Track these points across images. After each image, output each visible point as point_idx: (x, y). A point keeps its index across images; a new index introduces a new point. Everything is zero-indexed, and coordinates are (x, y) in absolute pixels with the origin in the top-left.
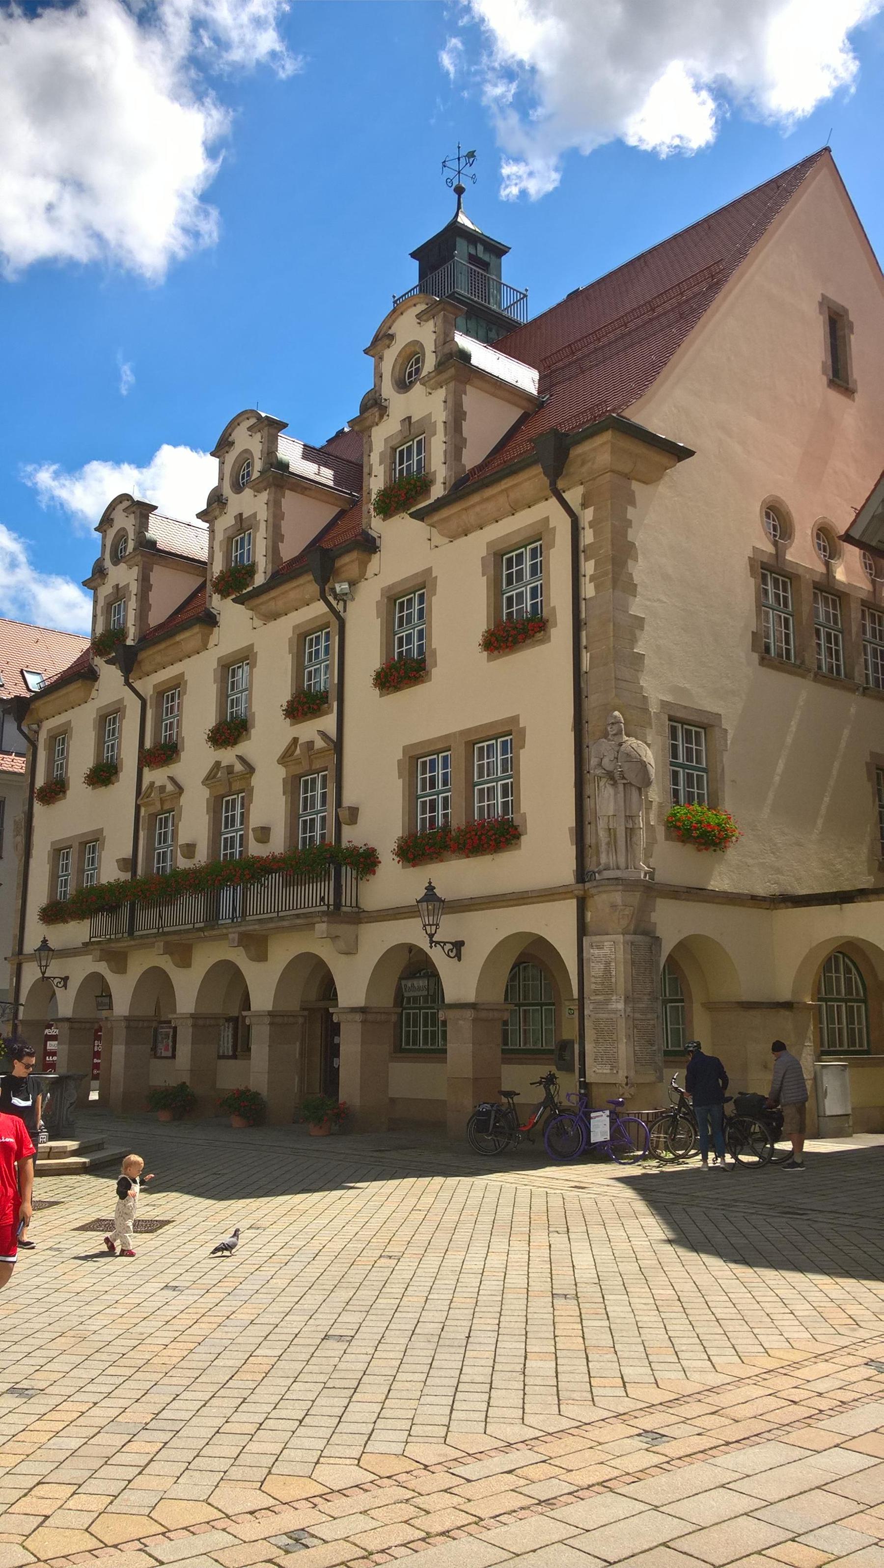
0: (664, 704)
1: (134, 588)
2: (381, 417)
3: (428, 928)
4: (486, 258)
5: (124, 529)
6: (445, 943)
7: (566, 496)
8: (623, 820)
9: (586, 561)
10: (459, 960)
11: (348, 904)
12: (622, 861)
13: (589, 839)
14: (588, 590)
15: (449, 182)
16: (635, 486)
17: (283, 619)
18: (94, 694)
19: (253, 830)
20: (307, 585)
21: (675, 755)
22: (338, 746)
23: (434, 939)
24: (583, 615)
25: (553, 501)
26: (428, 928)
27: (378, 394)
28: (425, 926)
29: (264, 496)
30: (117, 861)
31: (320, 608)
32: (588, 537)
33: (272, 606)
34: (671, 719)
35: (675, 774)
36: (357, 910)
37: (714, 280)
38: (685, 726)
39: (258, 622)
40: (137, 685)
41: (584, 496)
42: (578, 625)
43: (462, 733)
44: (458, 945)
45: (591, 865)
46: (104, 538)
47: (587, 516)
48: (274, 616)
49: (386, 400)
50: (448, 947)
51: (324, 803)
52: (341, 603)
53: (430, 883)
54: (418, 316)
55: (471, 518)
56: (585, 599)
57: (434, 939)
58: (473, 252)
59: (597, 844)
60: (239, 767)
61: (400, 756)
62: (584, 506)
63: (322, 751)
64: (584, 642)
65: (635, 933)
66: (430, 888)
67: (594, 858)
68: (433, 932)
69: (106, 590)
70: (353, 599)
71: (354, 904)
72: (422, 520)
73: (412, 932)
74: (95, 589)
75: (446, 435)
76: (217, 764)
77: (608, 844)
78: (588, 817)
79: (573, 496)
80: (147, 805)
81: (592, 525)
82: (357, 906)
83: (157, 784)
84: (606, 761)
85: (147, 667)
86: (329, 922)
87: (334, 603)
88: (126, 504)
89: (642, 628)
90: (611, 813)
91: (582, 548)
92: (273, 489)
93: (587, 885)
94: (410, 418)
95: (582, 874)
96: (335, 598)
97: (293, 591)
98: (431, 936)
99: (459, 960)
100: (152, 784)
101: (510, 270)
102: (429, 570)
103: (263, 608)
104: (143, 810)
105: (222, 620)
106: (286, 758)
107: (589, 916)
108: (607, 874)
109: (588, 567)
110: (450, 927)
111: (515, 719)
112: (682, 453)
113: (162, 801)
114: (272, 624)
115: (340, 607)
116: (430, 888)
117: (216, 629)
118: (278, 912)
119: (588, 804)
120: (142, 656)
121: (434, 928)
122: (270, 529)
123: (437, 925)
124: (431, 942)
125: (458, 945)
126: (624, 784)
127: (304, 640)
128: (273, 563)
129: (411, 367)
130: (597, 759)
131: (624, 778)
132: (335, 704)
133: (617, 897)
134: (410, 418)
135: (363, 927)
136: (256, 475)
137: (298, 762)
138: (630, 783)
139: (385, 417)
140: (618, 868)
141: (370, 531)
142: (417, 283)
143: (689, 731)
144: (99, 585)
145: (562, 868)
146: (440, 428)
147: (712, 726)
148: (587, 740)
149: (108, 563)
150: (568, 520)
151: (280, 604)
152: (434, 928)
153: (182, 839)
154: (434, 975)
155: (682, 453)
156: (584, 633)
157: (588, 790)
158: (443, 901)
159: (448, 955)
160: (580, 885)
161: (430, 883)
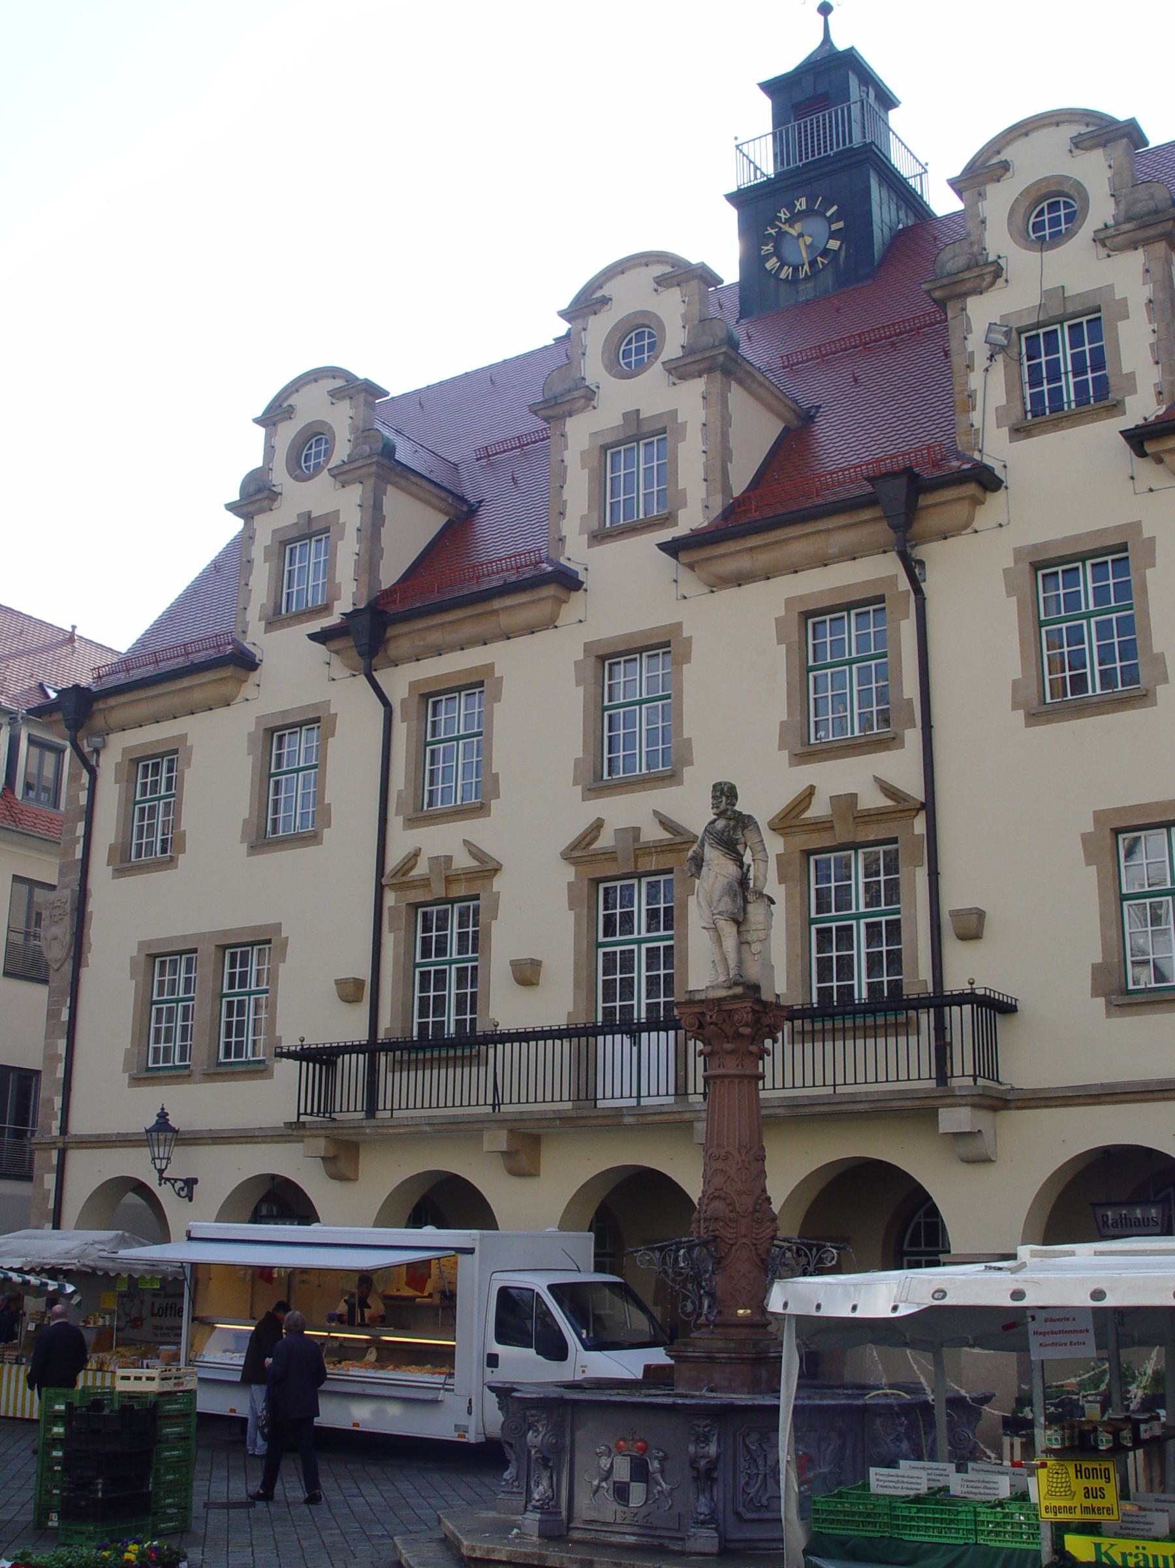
3: (158, 1161)
6: (176, 1180)
10: (191, 1200)
26: (158, 1161)
28: (154, 1159)
44: (191, 1183)
50: (180, 1184)
53: (163, 1109)
66: (163, 1115)
73: (137, 1164)
98: (161, 1171)
99: (191, 1200)
110: (183, 1162)
116: (163, 1115)
121: (164, 1161)
123: (169, 1159)
124: (161, 1178)
125: (191, 1183)
152: (164, 1161)
158: (177, 1132)
159: (179, 1195)
161: (163, 1109)
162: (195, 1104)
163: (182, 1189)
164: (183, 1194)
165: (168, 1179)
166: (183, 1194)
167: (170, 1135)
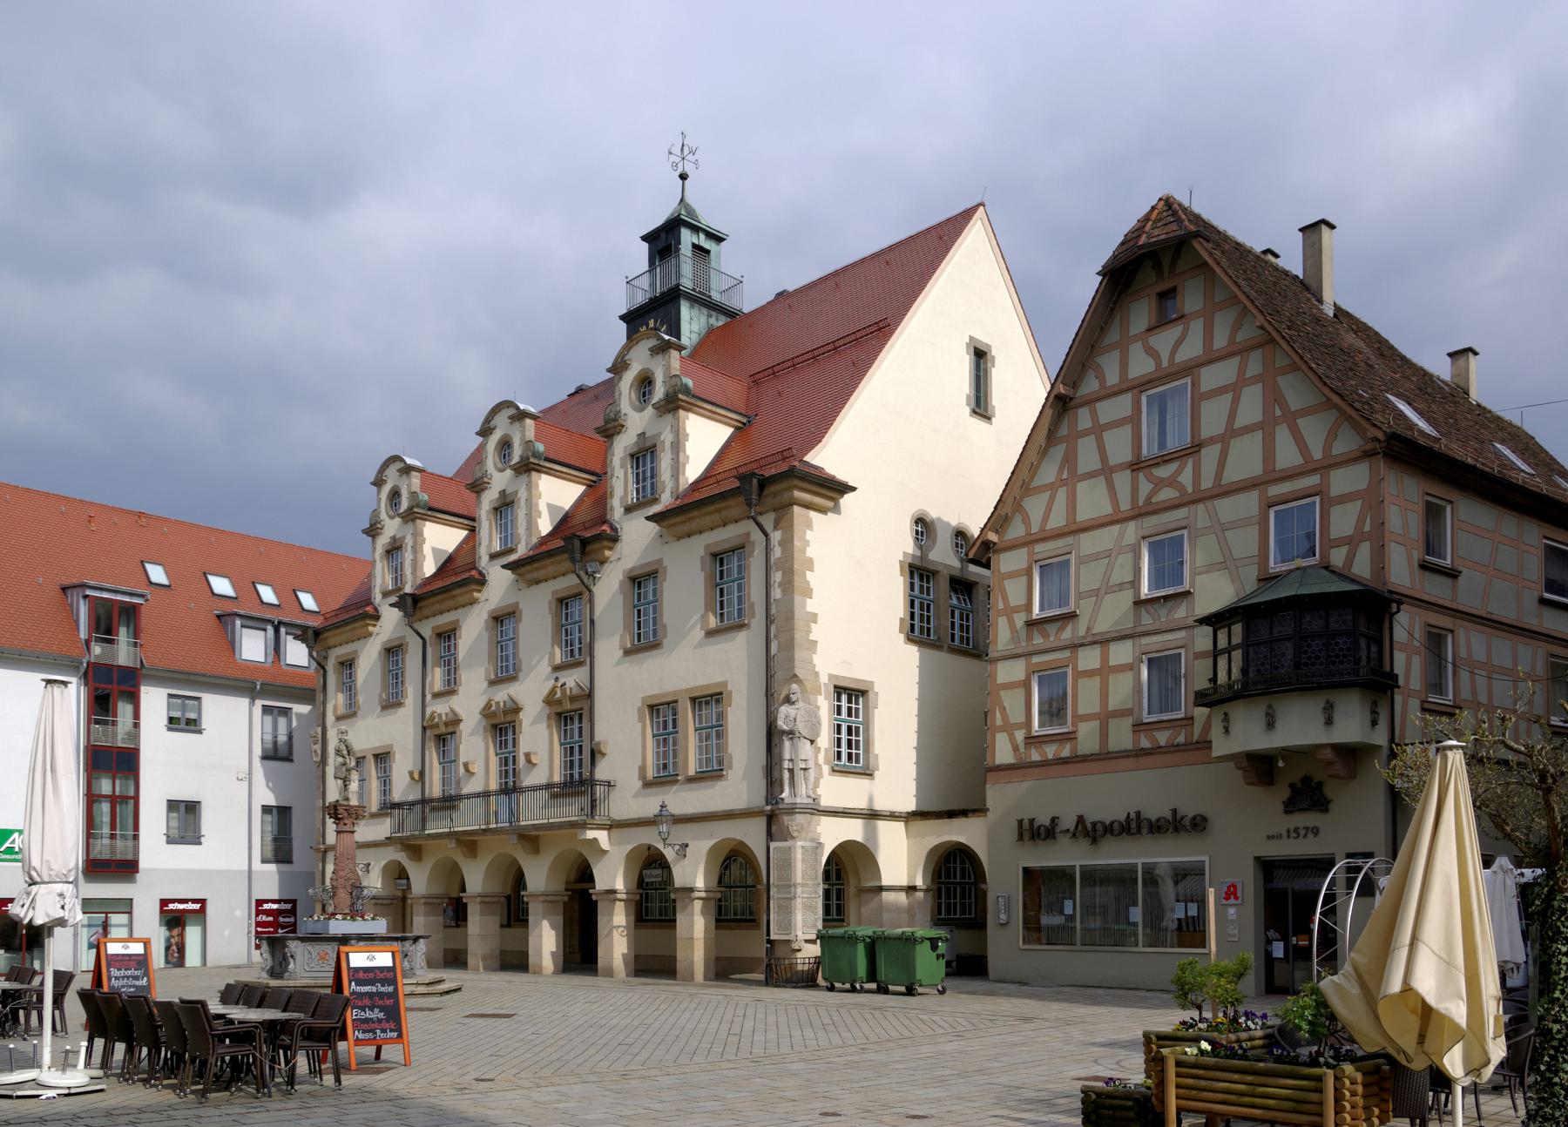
0: (831, 677)
22: (589, 695)
33: (535, 575)
34: (836, 687)
35: (839, 726)
37: (879, 331)
39: (522, 585)
42: (769, 620)
43: (686, 690)
48: (537, 582)
51: (580, 735)
54: (651, 350)
55: (693, 525)
69: (383, 540)
97: (551, 567)
101: (725, 258)
103: (529, 576)
111: (725, 684)
114: (534, 587)
127: (563, 602)
143: (852, 695)
153: (462, 760)
157: (775, 739)
162: (684, 800)
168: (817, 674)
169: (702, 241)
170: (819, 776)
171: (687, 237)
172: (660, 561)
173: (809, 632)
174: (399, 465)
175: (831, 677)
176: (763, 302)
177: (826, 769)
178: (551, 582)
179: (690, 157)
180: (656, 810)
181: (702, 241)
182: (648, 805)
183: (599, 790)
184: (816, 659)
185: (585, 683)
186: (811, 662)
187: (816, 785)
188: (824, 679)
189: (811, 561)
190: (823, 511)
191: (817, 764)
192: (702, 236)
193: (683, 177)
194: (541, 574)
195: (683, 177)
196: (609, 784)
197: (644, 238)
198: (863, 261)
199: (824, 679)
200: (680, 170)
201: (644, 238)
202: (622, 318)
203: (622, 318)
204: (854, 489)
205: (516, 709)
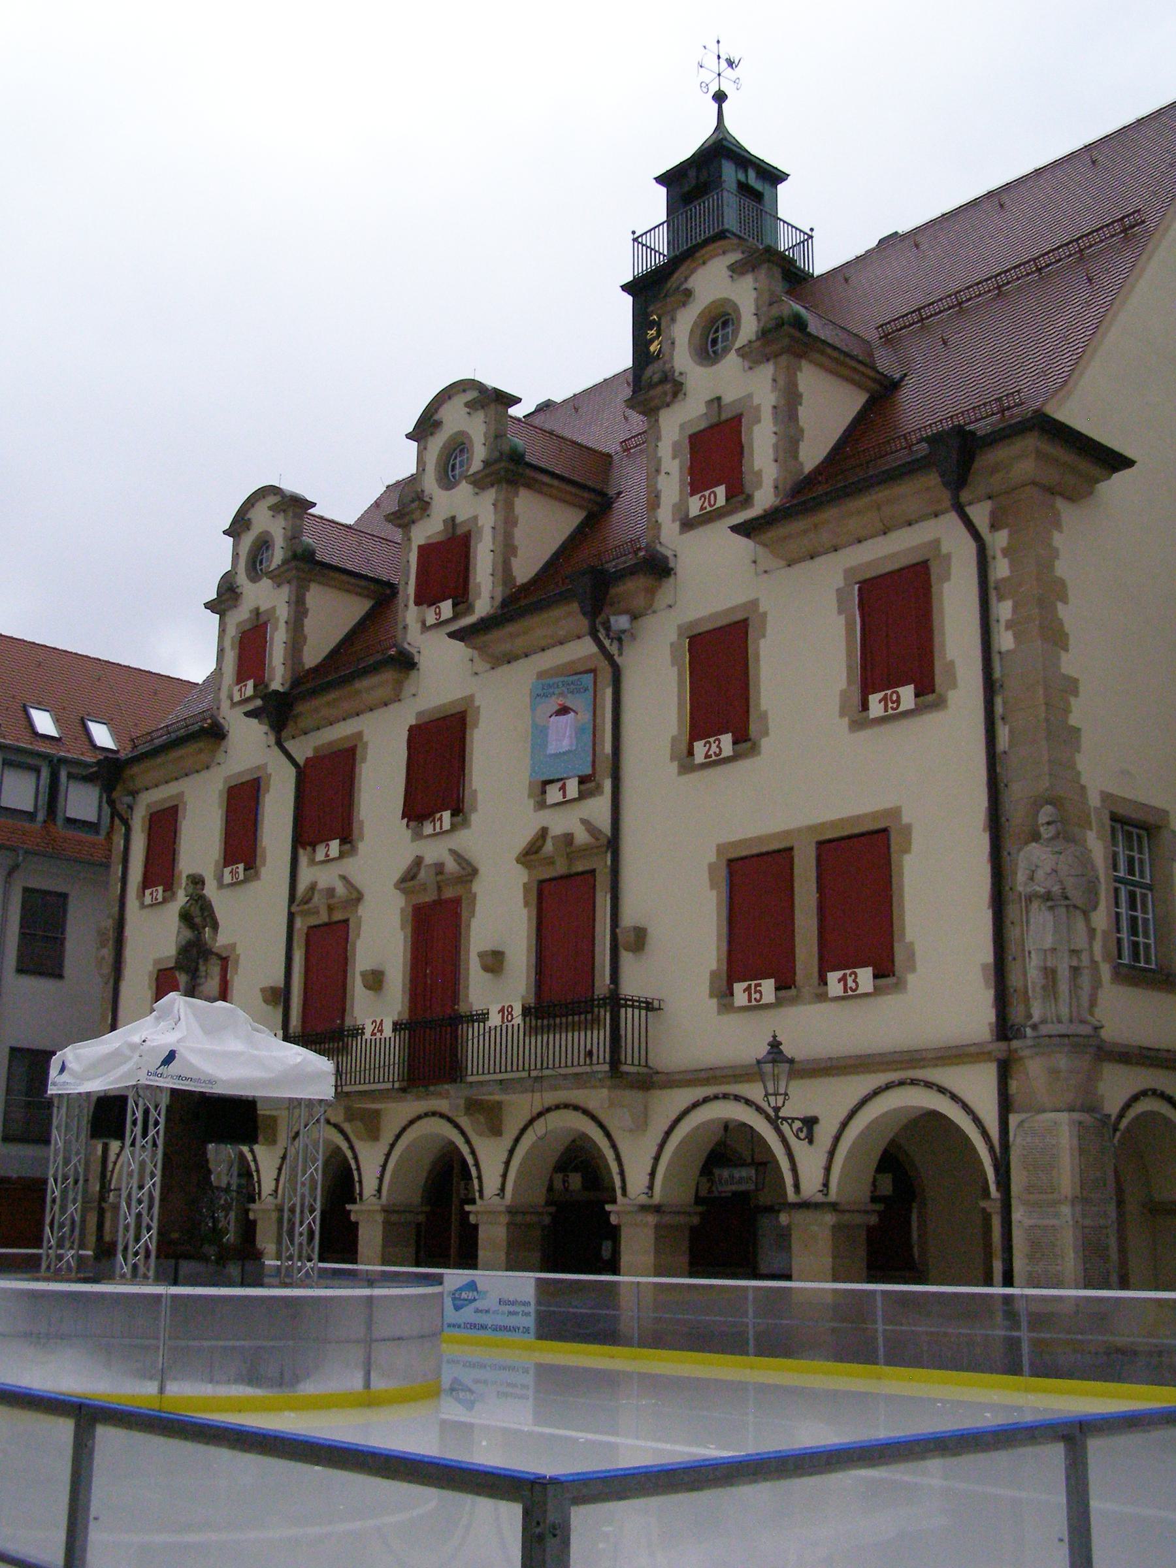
0: (1106, 797)
1: (283, 613)
2: (675, 395)
3: (772, 1099)
4: (758, 186)
5: (267, 533)
6: (793, 1119)
7: (969, 510)
8: (1066, 954)
9: (1000, 599)
10: (811, 1142)
11: (636, 1062)
12: (1064, 1011)
13: (1014, 979)
14: (1005, 640)
15: (705, 86)
16: (1060, 503)
17: (523, 663)
18: (220, 756)
19: (481, 955)
20: (569, 617)
21: (1115, 868)
22: (614, 843)
23: (781, 1114)
24: (997, 674)
25: (952, 518)
27: (668, 366)
28: (766, 1096)
29: (490, 495)
30: (263, 990)
31: (585, 648)
32: (1001, 569)
33: (506, 647)
36: (644, 1070)
38: (1126, 828)
39: (481, 665)
40: (288, 745)
41: (993, 514)
42: (990, 687)
43: (811, 829)
45: (1016, 1014)
46: (235, 546)
47: (998, 540)
48: (510, 659)
49: (681, 374)
52: (616, 643)
53: (775, 1037)
56: (1000, 653)
57: (781, 1114)
58: (741, 177)
59: (1026, 987)
60: (451, 866)
61: (712, 857)
62: (994, 527)
63: (586, 851)
64: (999, 709)
65: (1082, 1110)
66: (775, 1045)
67: (1022, 1008)
68: (780, 1104)
69: (241, 615)
70: (633, 637)
71: (643, 1062)
72: (748, 536)
74: (222, 614)
75: (775, 424)
76: (418, 861)
77: (1044, 988)
78: (1012, 949)
79: (980, 514)
80: (305, 914)
81: (1006, 552)
82: (646, 1066)
83: (322, 884)
84: (1040, 874)
85: (304, 723)
86: (609, 1088)
87: (607, 642)
88: (272, 500)
89: (1075, 692)
90: (1048, 946)
91: (992, 584)
92: (504, 486)
93: (1015, 1044)
94: (719, 399)
95: (1004, 1029)
96: (608, 636)
97: (539, 626)
99: (811, 1142)
100: (313, 887)
101: (790, 203)
102: (754, 603)
104: (299, 923)
105: (423, 661)
106: (531, 854)
107: (1013, 1086)
108: (1044, 1030)
109: (1003, 610)
110: (802, 1099)
112: (1116, 462)
113: (330, 909)
114: (506, 668)
115: (613, 649)
116: (775, 1045)
117: (414, 673)
118: (530, 1070)
119: (1013, 933)
120: (300, 708)
121: (780, 1099)
122: (500, 538)
126: (1067, 906)
128: (505, 584)
129: (716, 331)
130: (1028, 872)
131: (1067, 898)
132: (607, 785)
133: (1062, 1061)
134: (719, 399)
135: (656, 1094)
136: (476, 465)
137: (550, 861)
138: (1075, 907)
139: (680, 396)
140: (1059, 1021)
141: (658, 547)
142: (665, 218)
144: (230, 608)
145: (975, 1017)
146: (767, 415)
147: (1160, 827)
148: (1009, 844)
149: (242, 579)
150: (971, 546)
151: (520, 643)
152: (780, 1099)
154: (764, 1163)
155: (1116, 462)
156: (999, 700)
157: (1012, 911)
158: (791, 1061)
160: (1003, 1045)
161: (775, 1037)
162: (819, 1024)
163: (801, 1130)
164: (802, 1135)
165: (785, 1119)
166: (802, 1135)
167: (785, 1067)
168: (1083, 788)
169: (752, 179)
170: (1097, 985)
171: (730, 173)
172: (754, 603)
173: (1066, 711)
174: (272, 500)
175: (1106, 797)
176: (860, 251)
177: (1106, 971)
178: (535, 658)
179: (728, 72)
180: (761, 1050)
181: (752, 179)
182: (735, 1038)
183: (628, 1016)
184: (1083, 763)
185: (604, 823)
186: (1072, 765)
187: (1093, 1003)
188: (1094, 801)
189: (1062, 583)
190: (1072, 497)
191: (1094, 962)
192: (752, 174)
193: (720, 97)
194: (520, 643)
195: (720, 97)
196: (649, 1006)
197: (661, 180)
198: (1038, 172)
199: (1094, 801)
200: (714, 89)
201: (661, 180)
202: (626, 288)
203: (626, 288)
204: (1127, 463)
205: (469, 872)
